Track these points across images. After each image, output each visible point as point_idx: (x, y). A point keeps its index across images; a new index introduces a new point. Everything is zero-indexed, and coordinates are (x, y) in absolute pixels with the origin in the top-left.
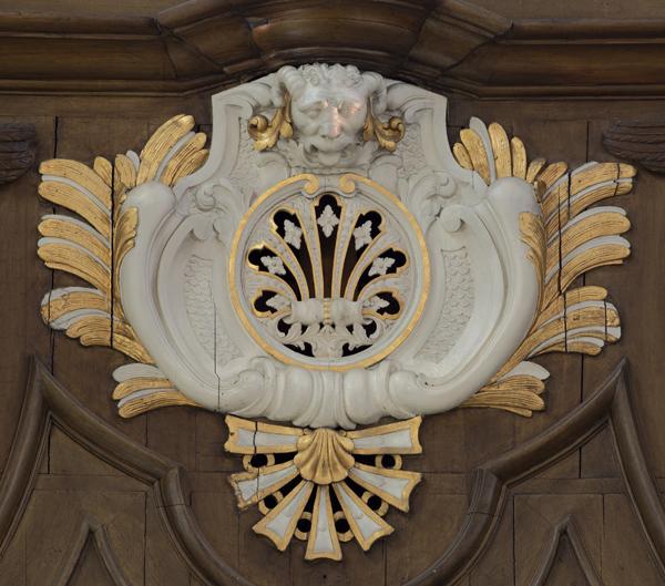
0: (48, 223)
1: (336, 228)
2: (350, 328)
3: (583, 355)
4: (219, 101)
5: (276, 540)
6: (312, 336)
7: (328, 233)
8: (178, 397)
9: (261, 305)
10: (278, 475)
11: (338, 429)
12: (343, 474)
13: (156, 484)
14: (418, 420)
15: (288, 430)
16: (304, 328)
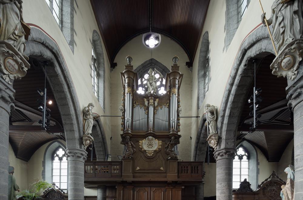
10: (148, 153)
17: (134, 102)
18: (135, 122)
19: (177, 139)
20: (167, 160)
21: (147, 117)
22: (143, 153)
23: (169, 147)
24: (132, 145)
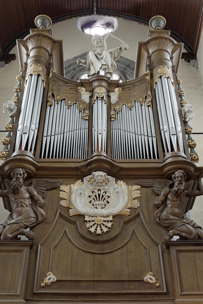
0: (61, 193)
1: (100, 193)
2: (102, 205)
3: (135, 208)
4: (84, 178)
5: (92, 231)
6: (97, 206)
7: (99, 194)
8: (78, 213)
9: (90, 202)
10: (92, 223)
11: (101, 217)
12: (102, 223)
13: (75, 224)
14: (112, 216)
15: (94, 217)
16: (96, 205)
17: (50, 94)
18: (49, 138)
19: (192, 182)
20: (168, 247)
21: (87, 126)
22: (74, 223)
23: (168, 202)
24: (32, 197)
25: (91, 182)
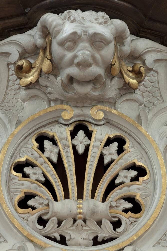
1: (87, 148)
2: (99, 223)
7: (81, 150)
16: (59, 223)
25: (31, 78)
